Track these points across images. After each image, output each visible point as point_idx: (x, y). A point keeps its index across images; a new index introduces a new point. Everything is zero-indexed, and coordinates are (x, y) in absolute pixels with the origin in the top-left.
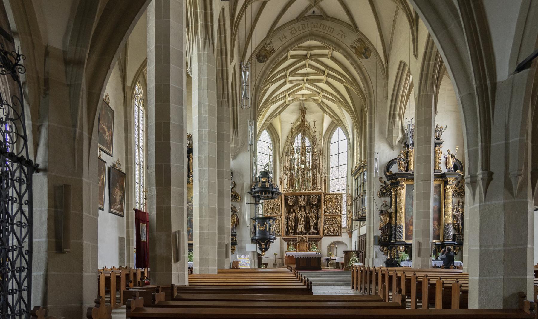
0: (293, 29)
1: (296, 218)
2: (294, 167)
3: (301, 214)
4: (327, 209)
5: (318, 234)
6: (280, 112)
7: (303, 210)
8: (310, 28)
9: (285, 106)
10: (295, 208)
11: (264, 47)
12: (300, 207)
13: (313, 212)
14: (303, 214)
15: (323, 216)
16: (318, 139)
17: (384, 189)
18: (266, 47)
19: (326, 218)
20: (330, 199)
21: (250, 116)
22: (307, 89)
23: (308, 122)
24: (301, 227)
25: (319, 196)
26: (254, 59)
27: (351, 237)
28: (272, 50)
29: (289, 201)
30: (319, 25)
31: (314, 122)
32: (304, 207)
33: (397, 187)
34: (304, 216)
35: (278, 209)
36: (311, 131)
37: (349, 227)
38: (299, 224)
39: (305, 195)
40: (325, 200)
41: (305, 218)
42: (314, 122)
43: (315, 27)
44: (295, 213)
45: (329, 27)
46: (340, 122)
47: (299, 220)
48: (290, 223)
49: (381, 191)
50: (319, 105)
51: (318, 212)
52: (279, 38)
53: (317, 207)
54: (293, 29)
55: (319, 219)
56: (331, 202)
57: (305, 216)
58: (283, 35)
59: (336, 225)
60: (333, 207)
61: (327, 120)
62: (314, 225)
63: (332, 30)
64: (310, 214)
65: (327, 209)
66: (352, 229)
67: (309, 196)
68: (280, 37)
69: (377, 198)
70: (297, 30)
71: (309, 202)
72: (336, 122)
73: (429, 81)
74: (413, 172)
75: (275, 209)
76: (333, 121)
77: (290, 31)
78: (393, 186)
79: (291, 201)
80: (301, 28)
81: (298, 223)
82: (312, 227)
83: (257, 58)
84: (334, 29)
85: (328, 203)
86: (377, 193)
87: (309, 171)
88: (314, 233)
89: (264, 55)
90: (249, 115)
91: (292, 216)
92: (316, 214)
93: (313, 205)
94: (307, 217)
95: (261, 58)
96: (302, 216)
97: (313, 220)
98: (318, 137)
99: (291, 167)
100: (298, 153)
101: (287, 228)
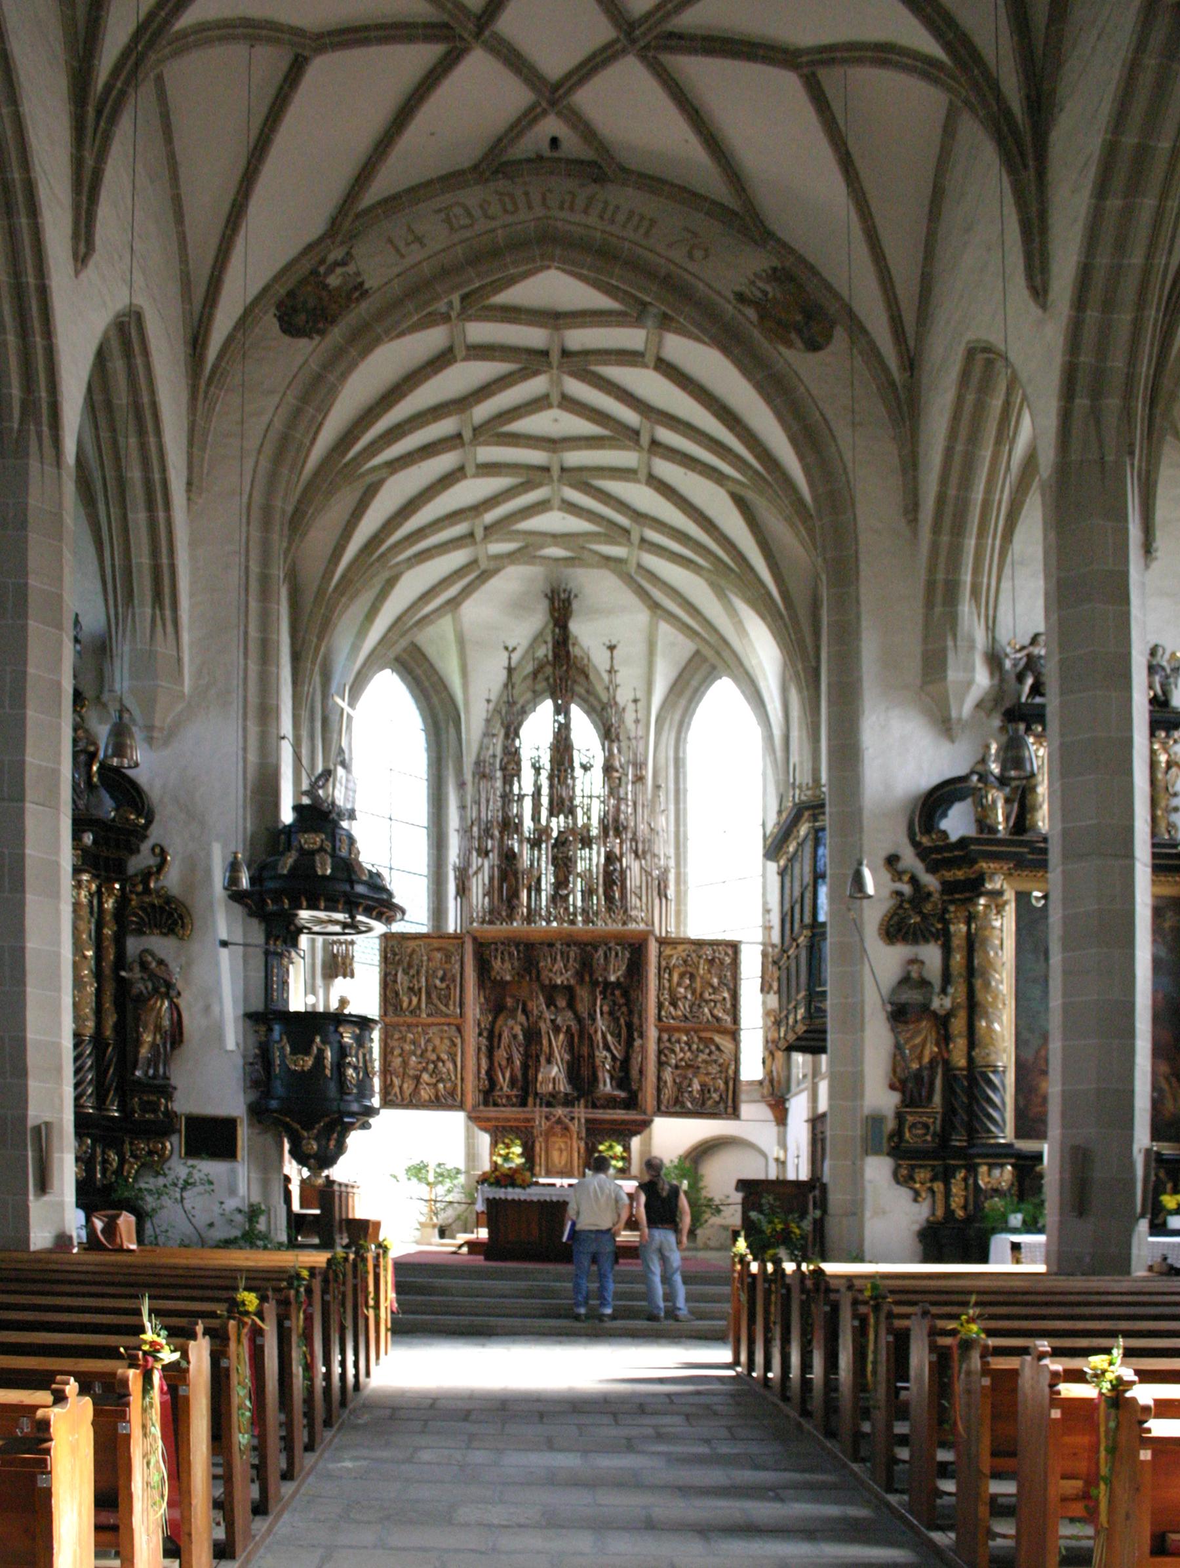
2: (518, 828)
3: (553, 1021)
4: (674, 1004)
5: (632, 1102)
6: (454, 603)
7: (562, 1003)
10: (524, 993)
12: (551, 993)
14: (566, 1019)
15: (652, 1033)
16: (629, 717)
19: (669, 1040)
20: (685, 961)
22: (571, 508)
23: (582, 648)
24: (553, 1075)
25: (636, 948)
27: (781, 1117)
29: (497, 964)
31: (612, 648)
32: (569, 991)
34: (569, 1027)
35: (448, 997)
36: (599, 689)
37: (771, 1081)
38: (543, 1060)
39: (570, 941)
40: (664, 963)
41: (572, 1035)
42: (612, 648)
44: (524, 1011)
46: (726, 654)
47: (545, 1042)
48: (501, 1054)
50: (628, 579)
51: (631, 1012)
53: (625, 994)
56: (692, 977)
57: (569, 1027)
59: (714, 1069)
60: (701, 995)
62: (613, 1067)
65: (674, 1004)
66: (788, 1089)
67: (586, 945)
72: (708, 652)
79: (508, 965)
82: (607, 1076)
85: (676, 977)
87: (587, 842)
88: (611, 1103)
92: (622, 1021)
93: (607, 984)
96: (557, 1029)
97: (607, 1048)
98: (631, 707)
99: (509, 825)
100: (537, 770)
101: (490, 1072)
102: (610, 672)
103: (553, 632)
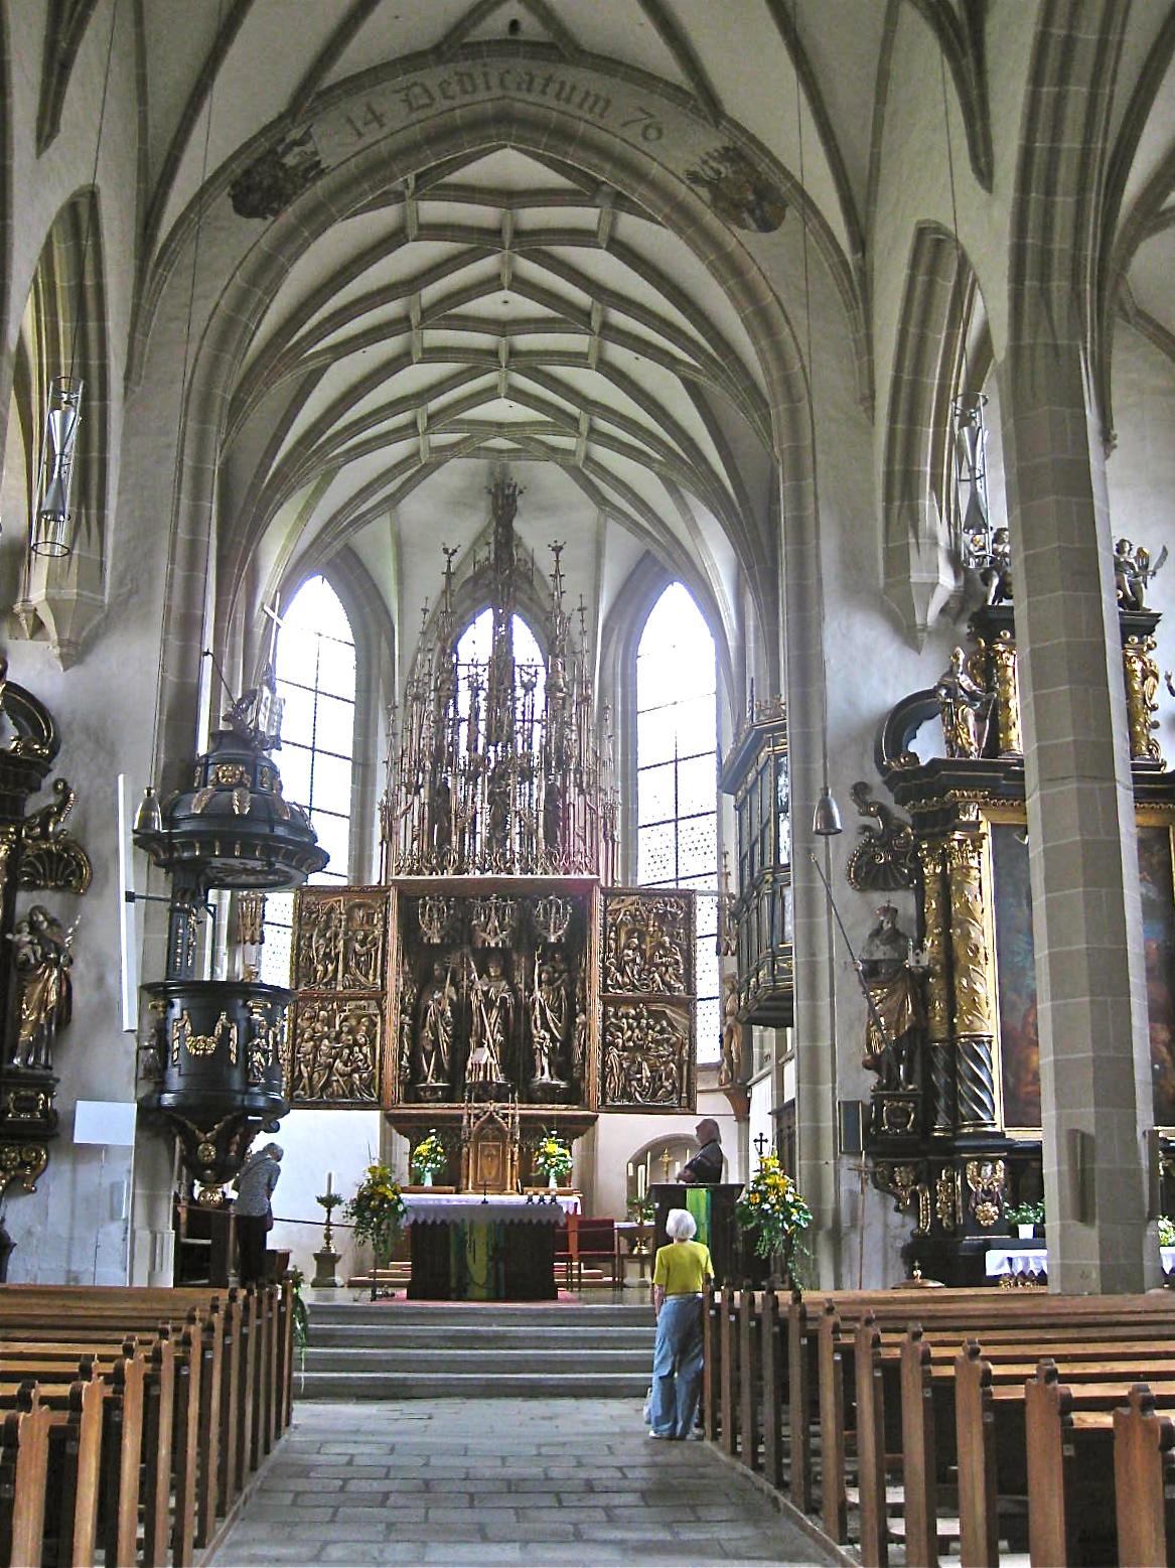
0: (417, 90)
1: (462, 1011)
3: (486, 993)
8: (497, 92)
9: (418, 470)
11: (272, 151)
12: (484, 957)
13: (550, 982)
14: (500, 990)
15: (597, 1007)
17: (883, 846)
18: (285, 153)
21: (174, 453)
23: (525, 550)
26: (223, 203)
28: (307, 170)
30: (538, 83)
31: (558, 550)
33: (945, 835)
34: (503, 1000)
42: (558, 550)
43: (519, 88)
45: (587, 94)
49: (865, 858)
51: (572, 982)
52: (350, 121)
53: (567, 959)
54: (417, 90)
55: (579, 1020)
58: (370, 109)
61: (621, 547)
62: (552, 1050)
63: (601, 104)
64: (531, 991)
68: (352, 116)
69: (845, 893)
70: (437, 93)
71: (526, 935)
72: (660, 555)
73: (1059, 285)
74: (1021, 763)
75: (352, 964)
76: (648, 552)
77: (402, 95)
78: (927, 831)
80: (455, 88)
81: (469, 1035)
83: (234, 197)
84: (608, 102)
86: (844, 867)
89: (269, 189)
90: (169, 446)
91: (441, 1002)
94: (518, 1005)
95: (255, 198)
96: (489, 1004)
97: (546, 1026)
98: (577, 616)
102: (554, 576)
103: (496, 532)
